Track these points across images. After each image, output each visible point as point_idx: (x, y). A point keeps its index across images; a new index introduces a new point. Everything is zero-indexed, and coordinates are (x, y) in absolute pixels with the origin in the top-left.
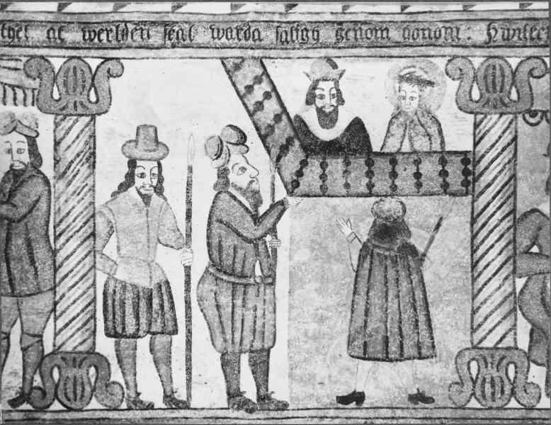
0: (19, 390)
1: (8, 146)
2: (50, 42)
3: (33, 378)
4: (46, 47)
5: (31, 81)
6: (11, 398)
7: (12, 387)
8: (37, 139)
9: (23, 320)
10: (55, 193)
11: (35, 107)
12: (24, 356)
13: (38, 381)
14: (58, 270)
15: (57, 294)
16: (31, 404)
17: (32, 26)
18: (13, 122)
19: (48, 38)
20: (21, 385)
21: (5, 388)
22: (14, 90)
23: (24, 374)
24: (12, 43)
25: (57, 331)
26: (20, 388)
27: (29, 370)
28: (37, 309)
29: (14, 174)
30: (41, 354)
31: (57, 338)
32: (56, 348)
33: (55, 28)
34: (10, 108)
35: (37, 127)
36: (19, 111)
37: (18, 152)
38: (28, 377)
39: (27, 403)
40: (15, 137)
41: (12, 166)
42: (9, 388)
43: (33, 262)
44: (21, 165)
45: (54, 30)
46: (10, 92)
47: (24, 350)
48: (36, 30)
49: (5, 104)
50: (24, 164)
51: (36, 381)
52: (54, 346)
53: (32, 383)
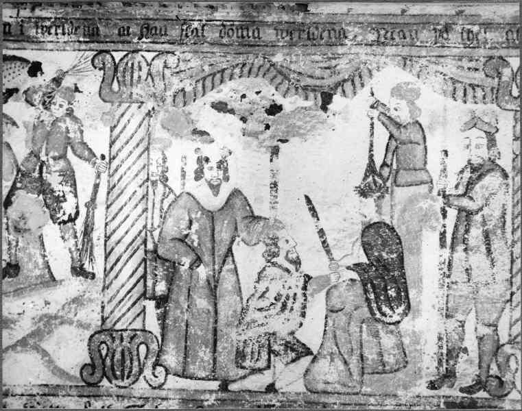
0: (476, 378)
1: (467, 142)
2: (509, 43)
3: (489, 366)
4: (505, 48)
5: (489, 80)
6: (468, 385)
7: (469, 374)
8: (497, 135)
9: (479, 310)
10: (513, 185)
11: (495, 105)
12: (479, 344)
13: (494, 370)
14: (515, 261)
15: (514, 284)
16: (488, 392)
17: (491, 28)
18: (473, 118)
19: (507, 39)
20: (477, 373)
21: (461, 375)
22: (474, 89)
23: (480, 362)
24: (471, 46)
25: (513, 320)
26: (476, 375)
27: (485, 358)
28: (492, 300)
29: (471, 168)
30: (495, 345)
31: (513, 327)
32: (513, 338)
33: (513, 30)
34: (470, 105)
35: (497, 123)
36: (480, 108)
37: (476, 148)
38: (484, 365)
39: (484, 391)
40: (475, 132)
41: (469, 160)
42: (465, 376)
43: (489, 251)
44: (479, 159)
45: (512, 32)
46: (470, 91)
47: (481, 339)
48: (494, 32)
49: (465, 102)
50: (482, 158)
51: (492, 369)
52: (510, 335)
53: (489, 372)
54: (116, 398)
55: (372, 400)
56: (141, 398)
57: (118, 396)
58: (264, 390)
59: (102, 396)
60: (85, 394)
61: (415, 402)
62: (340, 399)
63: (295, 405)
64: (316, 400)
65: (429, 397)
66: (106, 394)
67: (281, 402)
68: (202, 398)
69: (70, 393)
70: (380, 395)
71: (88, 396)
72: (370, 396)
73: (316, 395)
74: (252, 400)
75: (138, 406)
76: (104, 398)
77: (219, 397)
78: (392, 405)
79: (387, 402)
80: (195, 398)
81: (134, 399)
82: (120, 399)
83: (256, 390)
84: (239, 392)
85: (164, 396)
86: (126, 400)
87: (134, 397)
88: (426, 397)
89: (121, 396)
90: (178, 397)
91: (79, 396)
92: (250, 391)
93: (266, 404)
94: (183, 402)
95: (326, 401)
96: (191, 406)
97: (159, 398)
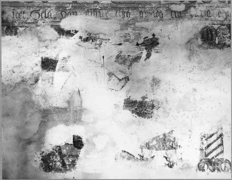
54: (27, 8)
55: (140, 6)
56: (38, 7)
57: (27, 7)
58: (93, 2)
59: (21, 7)
60: (12, 6)
61: (159, 6)
62: (126, 6)
63: (107, 9)
64: (116, 6)
65: (165, 4)
66: (22, 6)
67: (101, 7)
68: (66, 6)
69: (6, 5)
70: (143, 4)
71: (14, 7)
72: (139, 4)
73: (116, 4)
74: (88, 7)
75: (37, 10)
76: (22, 8)
77: (73, 6)
78: (148, 8)
79: (147, 6)
80: (63, 6)
81: (35, 7)
82: (29, 8)
83: (89, 2)
84: (82, 3)
85: (49, 6)
86: (31, 8)
87: (35, 6)
88: (163, 4)
89: (29, 7)
90: (55, 6)
91: (10, 6)
92: (87, 3)
93: (94, 8)
94: (57, 8)
95: (120, 6)
96: (61, 9)
97: (47, 7)
